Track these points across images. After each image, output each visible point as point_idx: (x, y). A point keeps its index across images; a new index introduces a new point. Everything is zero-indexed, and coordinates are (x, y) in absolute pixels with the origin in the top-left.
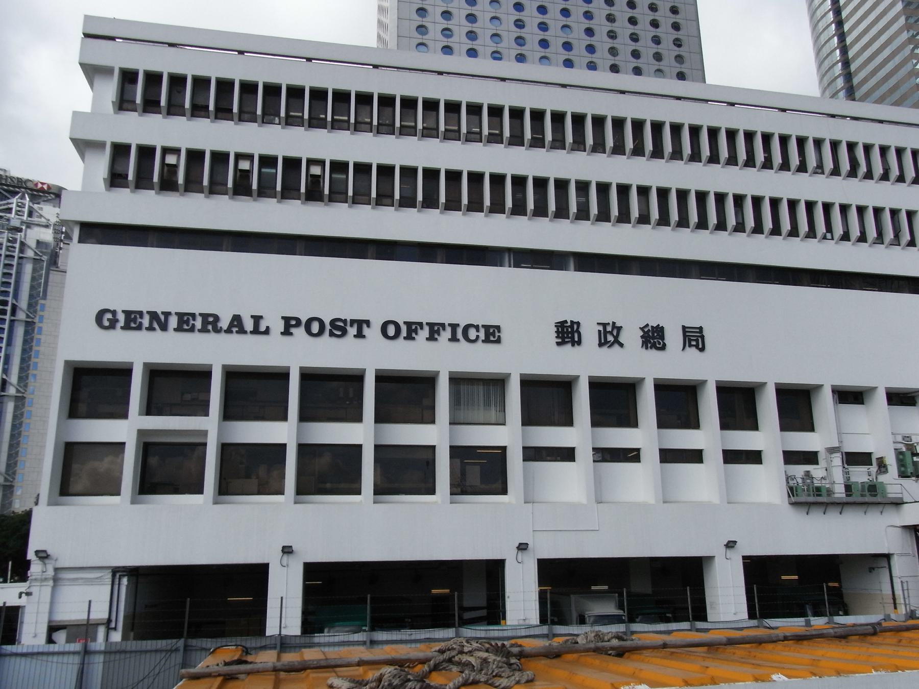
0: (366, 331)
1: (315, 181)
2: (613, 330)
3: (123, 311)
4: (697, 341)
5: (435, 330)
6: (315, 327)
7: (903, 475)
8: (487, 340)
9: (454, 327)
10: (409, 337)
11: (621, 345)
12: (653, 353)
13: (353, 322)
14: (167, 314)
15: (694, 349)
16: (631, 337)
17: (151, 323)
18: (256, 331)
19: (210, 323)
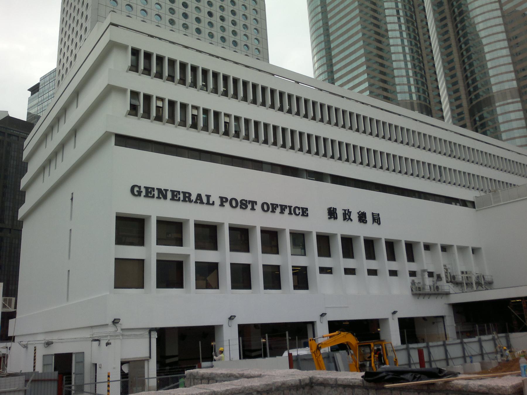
0: (255, 207)
1: (194, 117)
2: (348, 213)
3: (145, 187)
4: (378, 221)
5: (283, 208)
6: (234, 204)
7: (447, 282)
8: (303, 215)
9: (290, 207)
10: (273, 211)
11: (351, 220)
12: (362, 224)
13: (250, 201)
14: (166, 190)
15: (376, 223)
16: (355, 216)
17: (159, 195)
18: (208, 203)
19: (187, 197)
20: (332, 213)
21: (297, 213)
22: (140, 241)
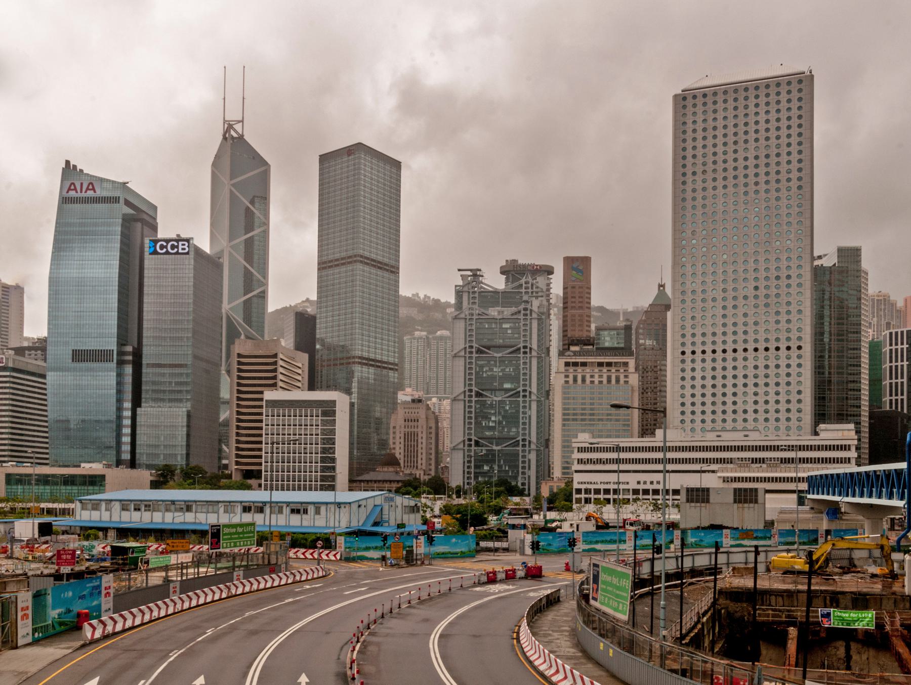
16: (648, 483)
20: (639, 483)
22: (581, 494)
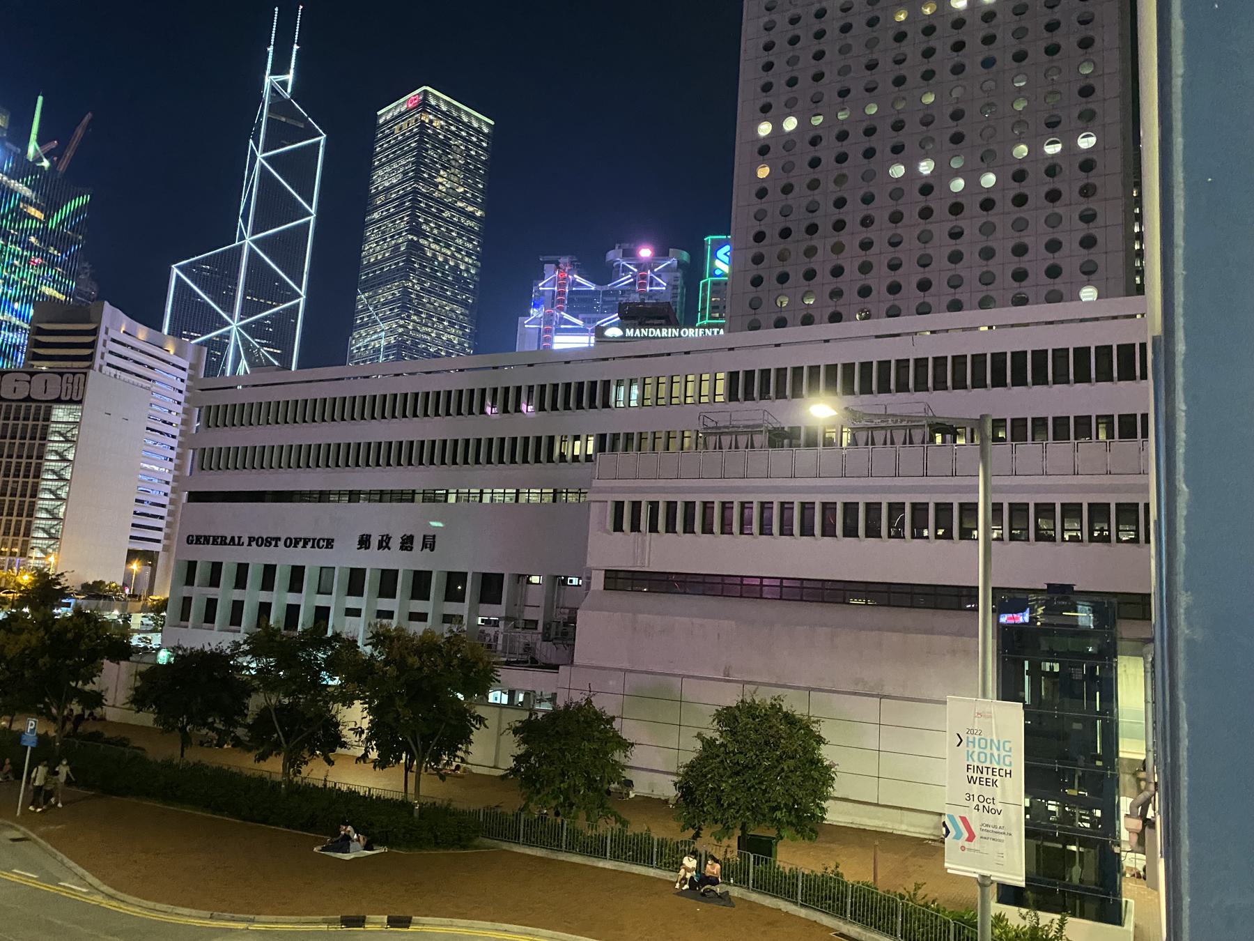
5: (306, 542)
8: (327, 547)
9: (314, 540)
10: (295, 546)
11: (389, 549)
14: (210, 536)
16: (395, 543)
18: (239, 544)
20: (364, 542)
21: (321, 545)
